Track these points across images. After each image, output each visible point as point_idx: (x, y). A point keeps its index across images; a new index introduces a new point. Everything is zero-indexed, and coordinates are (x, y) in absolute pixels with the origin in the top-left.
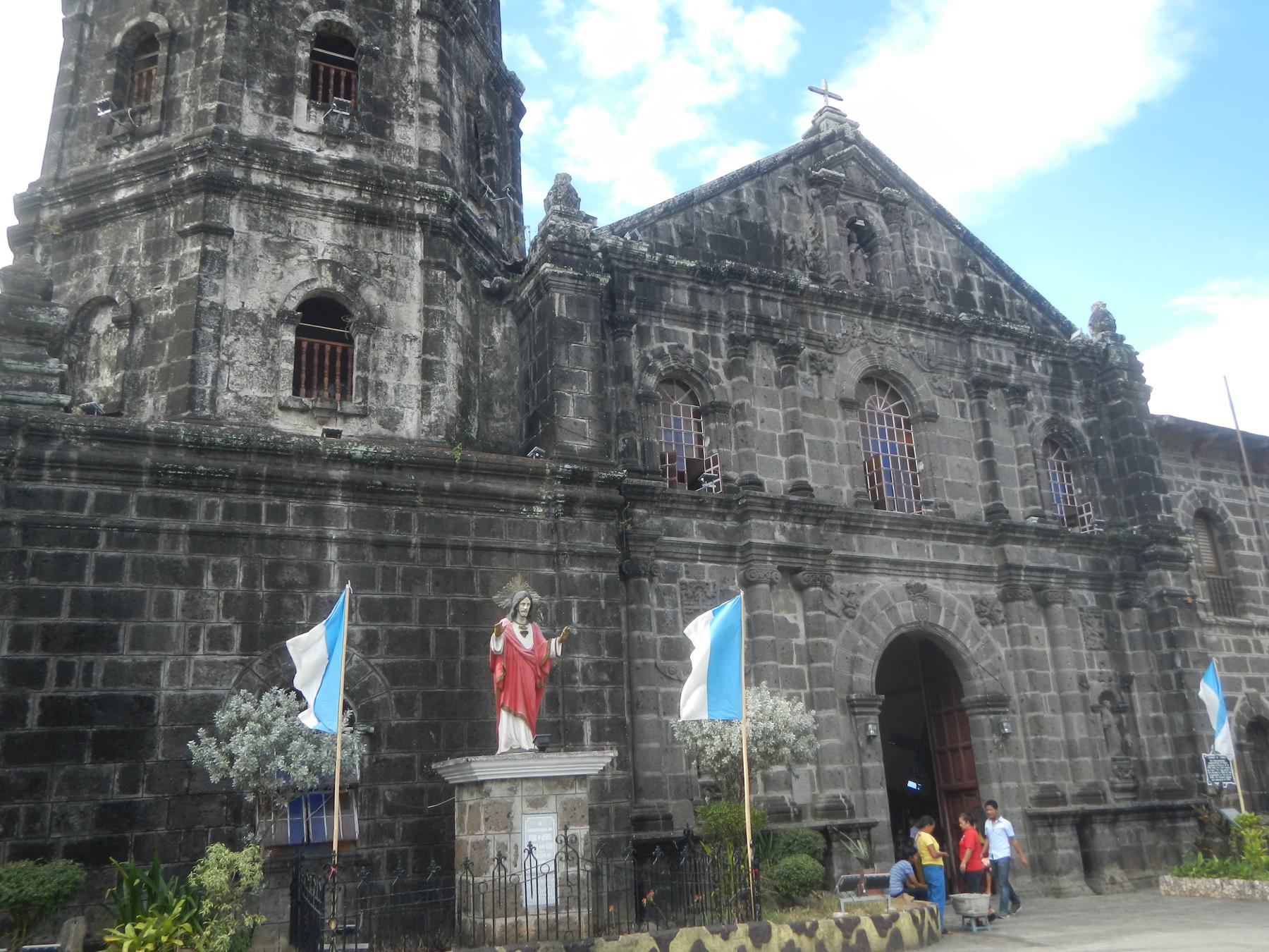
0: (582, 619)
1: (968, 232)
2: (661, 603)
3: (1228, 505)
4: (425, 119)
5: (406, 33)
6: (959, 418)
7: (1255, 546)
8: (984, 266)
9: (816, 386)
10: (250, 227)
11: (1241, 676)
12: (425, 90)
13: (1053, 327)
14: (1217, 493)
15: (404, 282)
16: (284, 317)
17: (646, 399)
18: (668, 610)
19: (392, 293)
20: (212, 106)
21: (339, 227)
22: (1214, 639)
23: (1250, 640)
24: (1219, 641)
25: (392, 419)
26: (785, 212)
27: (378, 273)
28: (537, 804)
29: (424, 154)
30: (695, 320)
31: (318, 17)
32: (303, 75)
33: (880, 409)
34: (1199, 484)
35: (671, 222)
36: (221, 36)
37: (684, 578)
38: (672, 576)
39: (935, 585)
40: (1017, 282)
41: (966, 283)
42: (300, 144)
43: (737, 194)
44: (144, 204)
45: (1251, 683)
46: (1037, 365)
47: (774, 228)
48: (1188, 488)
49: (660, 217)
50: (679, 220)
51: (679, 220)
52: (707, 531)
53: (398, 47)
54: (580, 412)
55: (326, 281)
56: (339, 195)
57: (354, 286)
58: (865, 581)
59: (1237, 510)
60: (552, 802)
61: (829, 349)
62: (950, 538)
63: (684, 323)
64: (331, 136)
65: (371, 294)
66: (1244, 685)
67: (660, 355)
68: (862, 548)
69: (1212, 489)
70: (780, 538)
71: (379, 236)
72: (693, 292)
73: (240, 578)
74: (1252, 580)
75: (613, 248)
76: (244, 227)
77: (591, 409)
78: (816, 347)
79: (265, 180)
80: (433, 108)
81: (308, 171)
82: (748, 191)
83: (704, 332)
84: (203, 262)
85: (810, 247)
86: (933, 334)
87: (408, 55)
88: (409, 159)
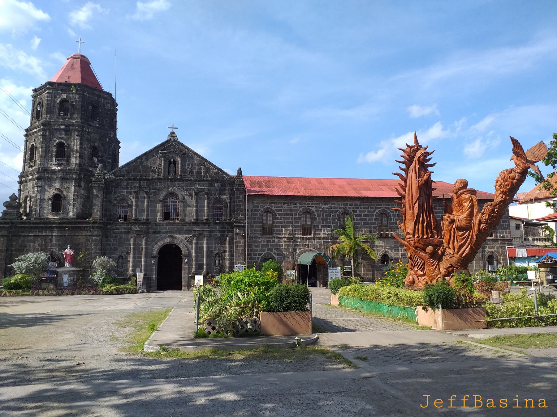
0: (94, 245)
1: (202, 157)
2: (114, 241)
3: (276, 210)
4: (76, 157)
5: (74, 140)
6: (191, 200)
7: (282, 219)
8: (206, 163)
9: (154, 198)
10: (45, 184)
11: (266, 248)
12: (77, 151)
13: (224, 175)
14: (273, 207)
15: (71, 189)
16: (50, 199)
17: (114, 205)
18: (115, 242)
19: (68, 192)
20: (39, 163)
21: (60, 181)
22: (260, 240)
23: (272, 240)
24: (262, 241)
25: (68, 214)
26: (153, 161)
27: (66, 189)
28: (66, 274)
29: (76, 164)
30: (127, 188)
31: (57, 141)
32: (54, 154)
33: (172, 200)
34: (267, 205)
35: (124, 169)
36: (41, 149)
37: (119, 237)
38: (116, 237)
39: (177, 236)
40: (215, 166)
41: (200, 169)
42: (54, 167)
43: (142, 159)
44: (31, 180)
45: (268, 250)
46: (216, 185)
47: (149, 165)
48: (263, 207)
49: (121, 168)
50: (126, 168)
51: (126, 168)
52: (124, 228)
53: (72, 143)
54: (97, 211)
55: (56, 192)
56: (60, 176)
57: (62, 192)
58: (159, 235)
59: (278, 211)
60: (68, 274)
61: (158, 190)
62: (182, 225)
63: (124, 189)
64: (59, 165)
65: (65, 193)
66: (266, 250)
67: (118, 197)
68: (160, 229)
69: (272, 206)
70: (138, 229)
71: (66, 182)
72: (128, 183)
73: (40, 241)
74: (279, 227)
75: (108, 178)
76: (44, 184)
77: (100, 210)
78: (155, 190)
79: (47, 175)
80: (78, 154)
81: (54, 172)
82: (144, 158)
83: (129, 190)
84: (37, 192)
85: (157, 168)
86: (187, 183)
87: (74, 144)
88: (73, 165)
